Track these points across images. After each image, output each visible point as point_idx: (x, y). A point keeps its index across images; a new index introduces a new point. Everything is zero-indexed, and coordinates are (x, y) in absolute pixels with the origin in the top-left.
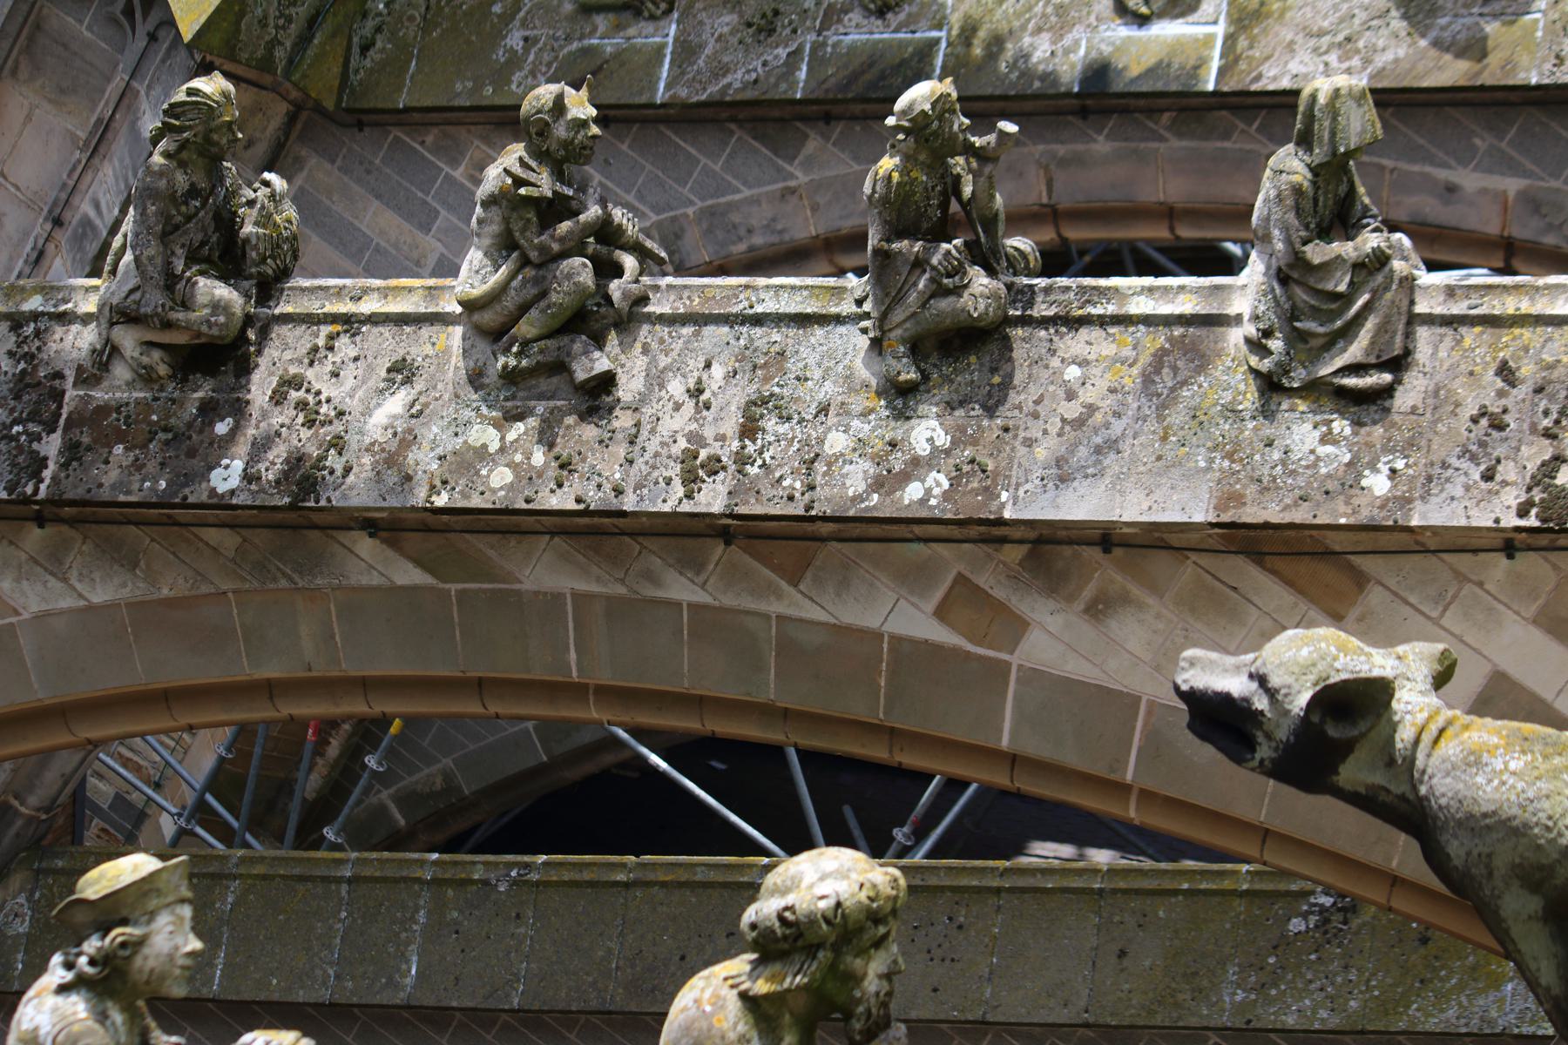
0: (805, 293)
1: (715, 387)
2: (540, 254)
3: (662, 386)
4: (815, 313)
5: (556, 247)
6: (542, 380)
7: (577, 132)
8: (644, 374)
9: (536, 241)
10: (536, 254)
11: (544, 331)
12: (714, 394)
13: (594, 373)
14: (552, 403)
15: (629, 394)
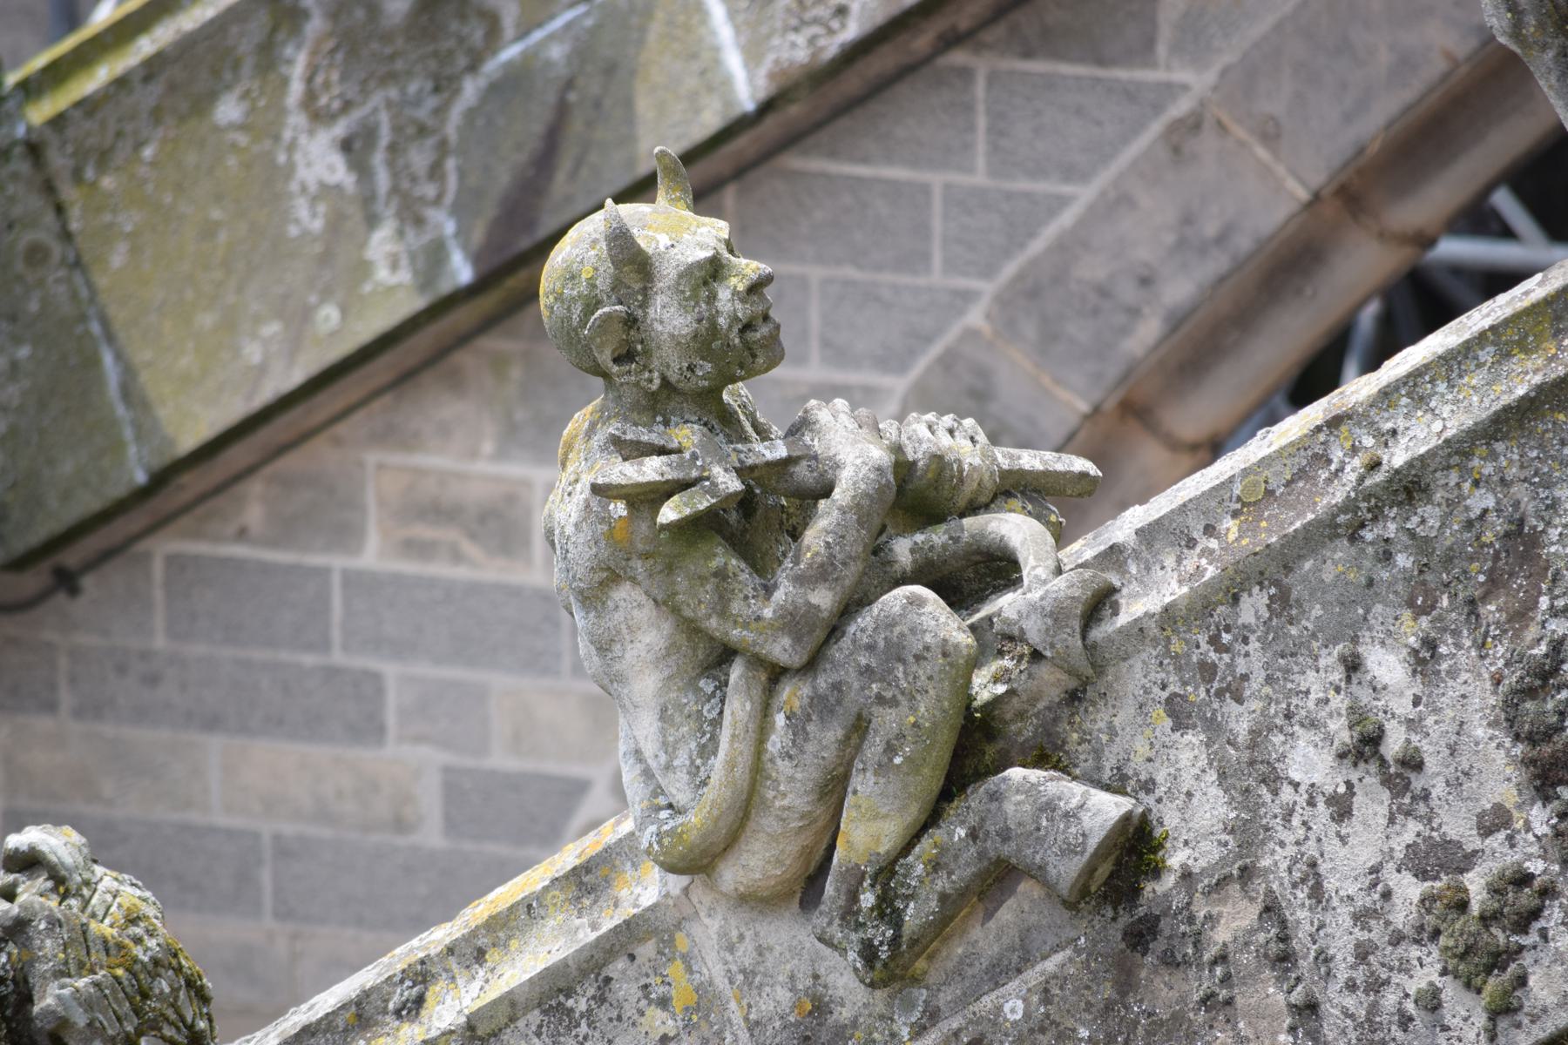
0: (1486, 355)
1: (1403, 707)
2: (797, 639)
3: (1273, 780)
4: (1540, 388)
5: (823, 599)
6: (976, 933)
7: (712, 298)
8: (1212, 776)
9: (768, 613)
10: (786, 641)
11: (914, 812)
12: (1412, 724)
13: (1093, 843)
14: (1033, 976)
15: (1205, 845)
